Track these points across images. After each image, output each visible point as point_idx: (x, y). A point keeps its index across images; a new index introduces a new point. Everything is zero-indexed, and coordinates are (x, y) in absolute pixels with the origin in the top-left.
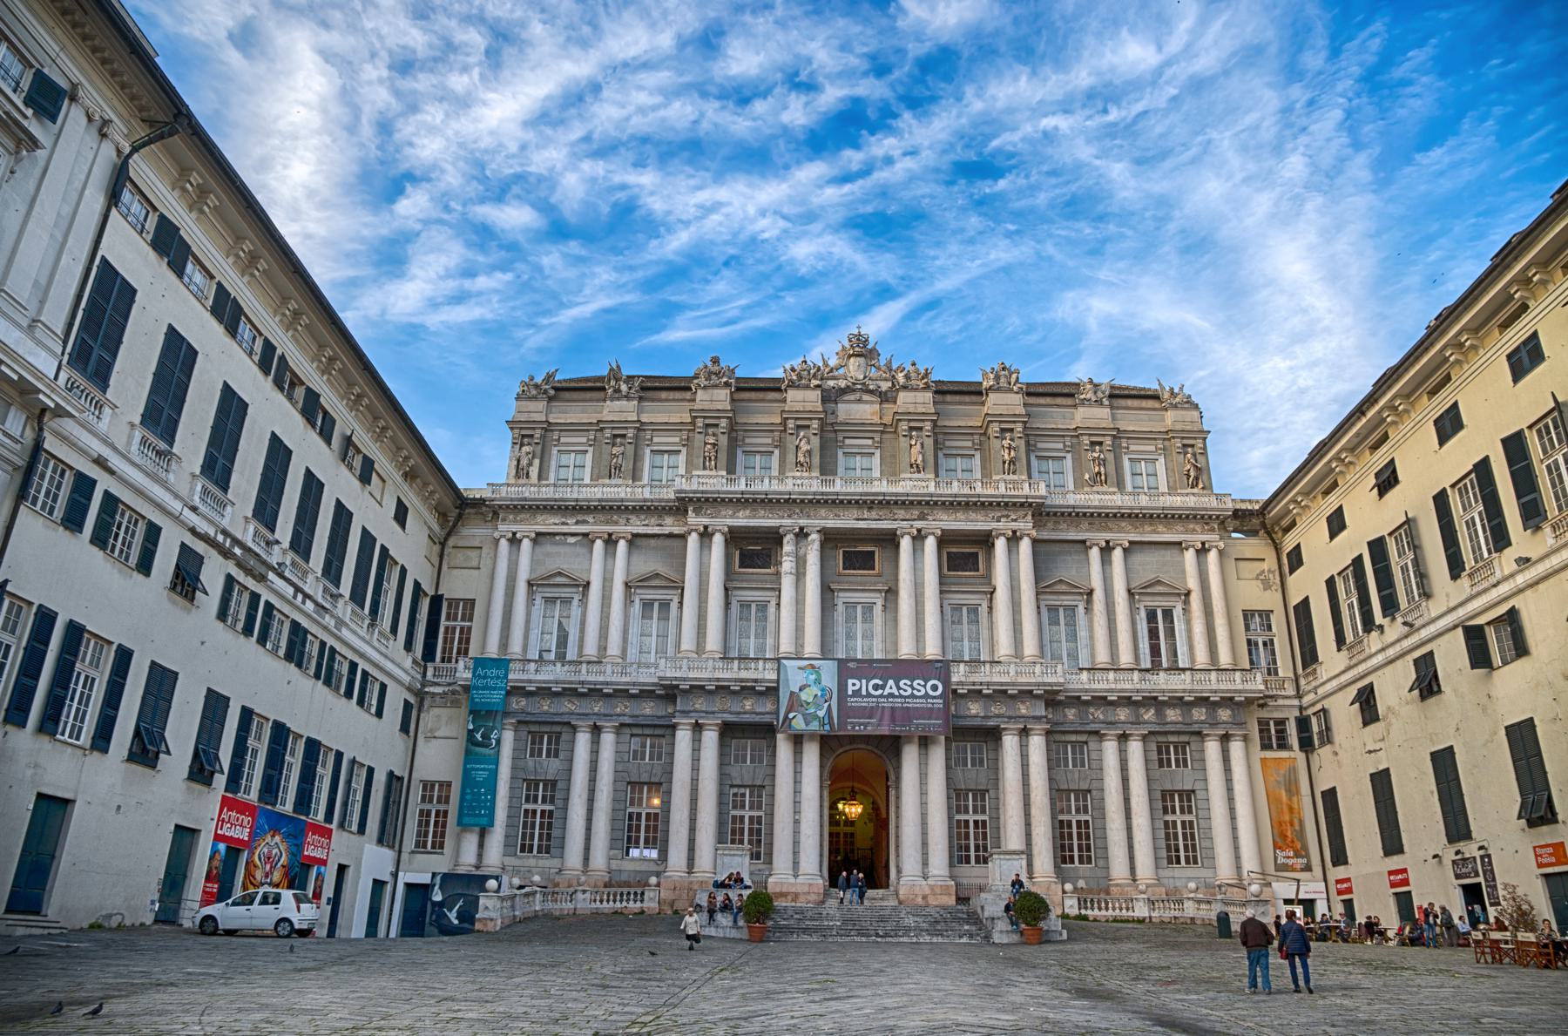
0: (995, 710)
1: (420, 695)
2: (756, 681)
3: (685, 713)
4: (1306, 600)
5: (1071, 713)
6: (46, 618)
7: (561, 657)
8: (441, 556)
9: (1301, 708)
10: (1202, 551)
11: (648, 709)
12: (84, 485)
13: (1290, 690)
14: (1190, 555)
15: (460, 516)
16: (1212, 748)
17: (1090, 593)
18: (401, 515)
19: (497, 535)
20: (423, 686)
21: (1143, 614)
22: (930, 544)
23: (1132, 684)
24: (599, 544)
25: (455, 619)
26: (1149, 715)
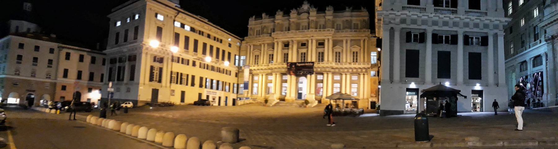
0: (323, 70)
1: (239, 71)
5: (337, 70)
6: (178, 73)
11: (270, 71)
12: (179, 58)
14: (362, 41)
16: (362, 76)
18: (230, 45)
22: (314, 42)
23: (348, 66)
24: (263, 46)
26: (350, 70)
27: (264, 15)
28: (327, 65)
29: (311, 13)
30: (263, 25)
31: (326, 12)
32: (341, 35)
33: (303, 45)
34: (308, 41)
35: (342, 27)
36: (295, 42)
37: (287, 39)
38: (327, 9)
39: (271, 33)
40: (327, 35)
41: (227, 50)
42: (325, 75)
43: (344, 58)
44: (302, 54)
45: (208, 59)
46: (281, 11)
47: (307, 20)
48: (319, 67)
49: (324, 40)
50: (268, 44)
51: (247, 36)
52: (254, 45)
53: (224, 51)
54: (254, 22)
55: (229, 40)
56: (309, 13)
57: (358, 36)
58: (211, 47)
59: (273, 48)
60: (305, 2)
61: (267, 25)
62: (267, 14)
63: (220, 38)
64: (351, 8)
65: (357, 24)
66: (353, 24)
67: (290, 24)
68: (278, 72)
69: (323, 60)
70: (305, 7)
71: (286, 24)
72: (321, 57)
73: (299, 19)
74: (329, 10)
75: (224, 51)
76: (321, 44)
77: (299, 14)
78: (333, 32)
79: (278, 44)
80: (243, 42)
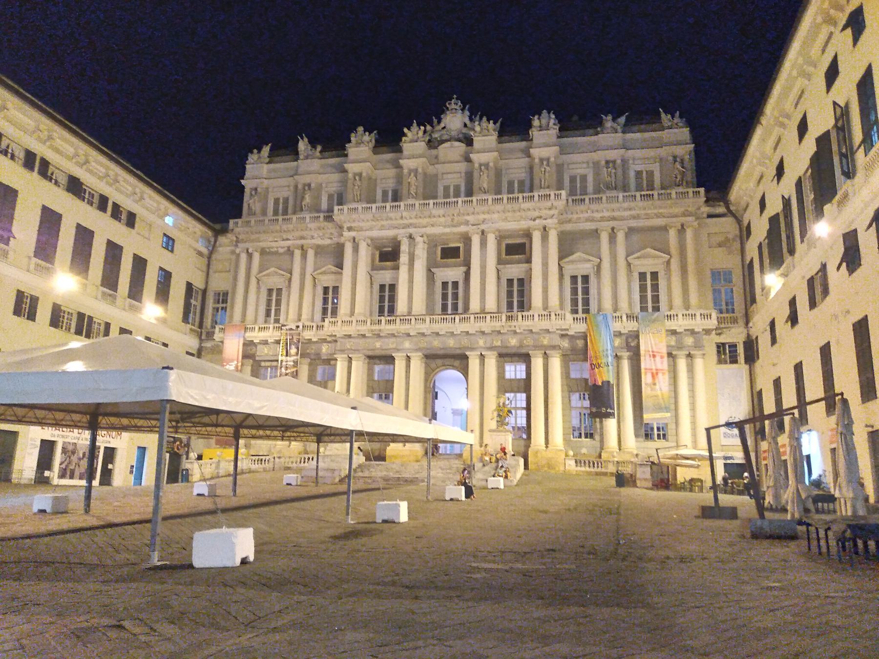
2: (380, 330)
3: (342, 351)
4: (752, 261)
7: (277, 321)
8: (209, 265)
9: (749, 335)
10: (682, 230)
13: (741, 322)
14: (672, 234)
15: (215, 242)
17: (599, 266)
18: (169, 243)
19: (238, 251)
20: (201, 344)
21: (636, 276)
24: (298, 253)
25: (218, 303)
27: (303, 145)
28: (545, 324)
29: (478, 142)
30: (302, 180)
31: (534, 133)
32: (589, 215)
33: (450, 253)
34: (467, 240)
35: (590, 188)
36: (419, 239)
37: (391, 233)
38: (536, 122)
39: (330, 210)
40: (539, 215)
41: (157, 260)
42: (537, 363)
43: (603, 293)
44: (445, 284)
45: (64, 284)
46: (368, 130)
47: (463, 167)
48: (515, 332)
49: (528, 235)
50: (319, 250)
51: (239, 215)
52: (263, 252)
53: (140, 264)
54: (265, 168)
55: (169, 220)
56: (469, 141)
57: (658, 216)
58: (84, 236)
59: (340, 266)
60: (454, 104)
61: (314, 180)
62: (313, 143)
63: (128, 204)
64: (622, 120)
65: (650, 174)
66: (632, 174)
67: (399, 179)
68: (356, 351)
69: (524, 305)
70: (454, 119)
71: (386, 177)
72: (517, 295)
73: (436, 160)
74: (541, 128)
75: (140, 264)
76: (517, 249)
77: (432, 144)
78: (561, 204)
79: (356, 249)
80: (222, 239)
